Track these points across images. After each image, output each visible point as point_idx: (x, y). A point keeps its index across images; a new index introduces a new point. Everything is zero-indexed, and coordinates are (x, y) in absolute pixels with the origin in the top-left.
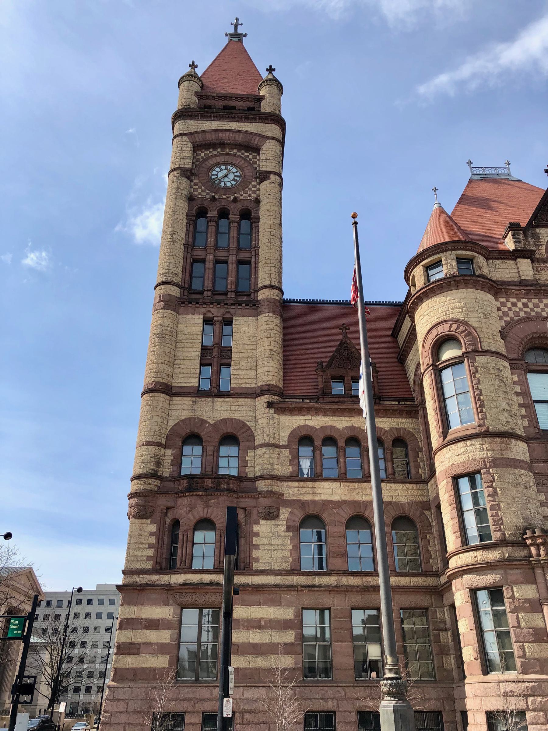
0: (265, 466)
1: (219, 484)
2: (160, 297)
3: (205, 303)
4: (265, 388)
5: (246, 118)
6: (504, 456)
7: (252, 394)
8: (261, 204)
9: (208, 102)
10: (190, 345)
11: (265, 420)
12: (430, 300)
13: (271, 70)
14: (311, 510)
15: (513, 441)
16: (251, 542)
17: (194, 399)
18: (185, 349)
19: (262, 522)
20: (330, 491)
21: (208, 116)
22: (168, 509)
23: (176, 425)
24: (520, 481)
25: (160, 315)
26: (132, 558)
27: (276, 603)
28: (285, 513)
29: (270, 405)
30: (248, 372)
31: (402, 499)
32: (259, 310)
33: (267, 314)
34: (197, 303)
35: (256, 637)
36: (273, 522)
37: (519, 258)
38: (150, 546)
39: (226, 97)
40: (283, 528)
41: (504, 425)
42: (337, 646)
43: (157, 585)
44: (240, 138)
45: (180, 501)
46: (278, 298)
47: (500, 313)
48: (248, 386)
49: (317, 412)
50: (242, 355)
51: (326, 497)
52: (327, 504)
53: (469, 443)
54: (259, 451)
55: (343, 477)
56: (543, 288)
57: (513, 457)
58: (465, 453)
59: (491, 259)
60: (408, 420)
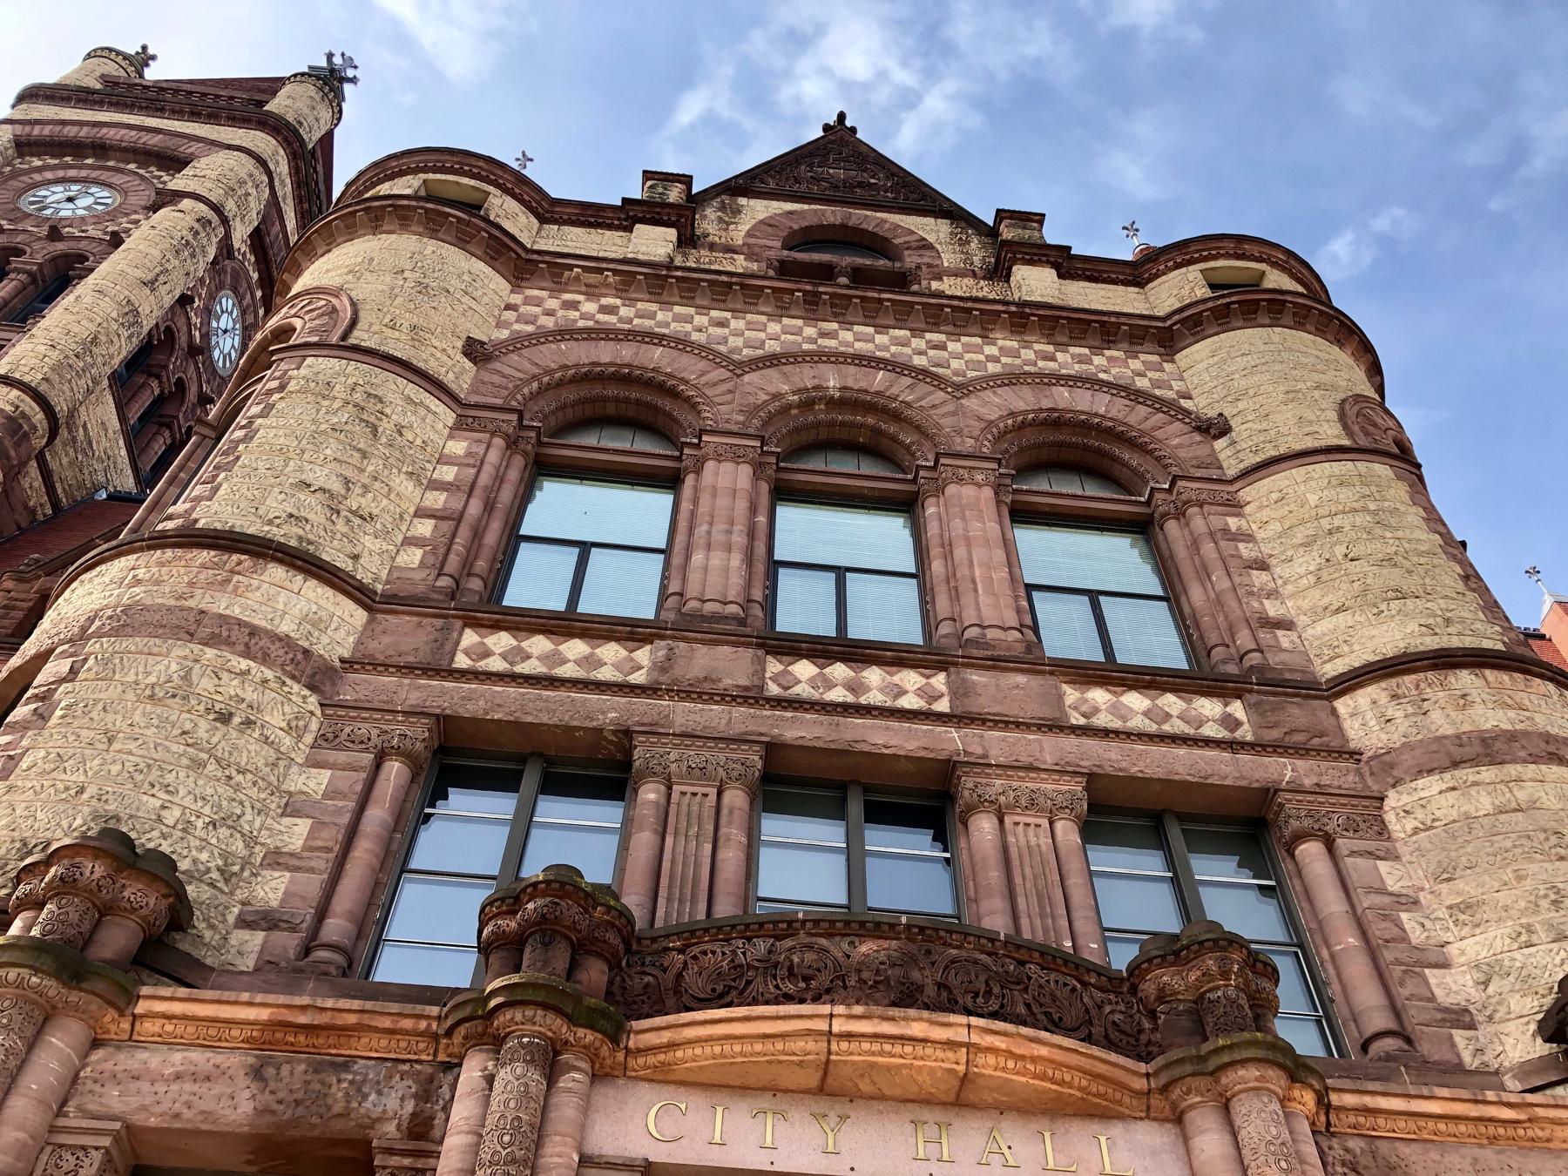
6: (191, 603)
15: (277, 572)
24: (205, 684)
37: (643, 221)
41: (270, 522)
46: (8, 408)
47: (510, 315)
56: (679, 274)
57: (236, 612)
59: (555, 222)
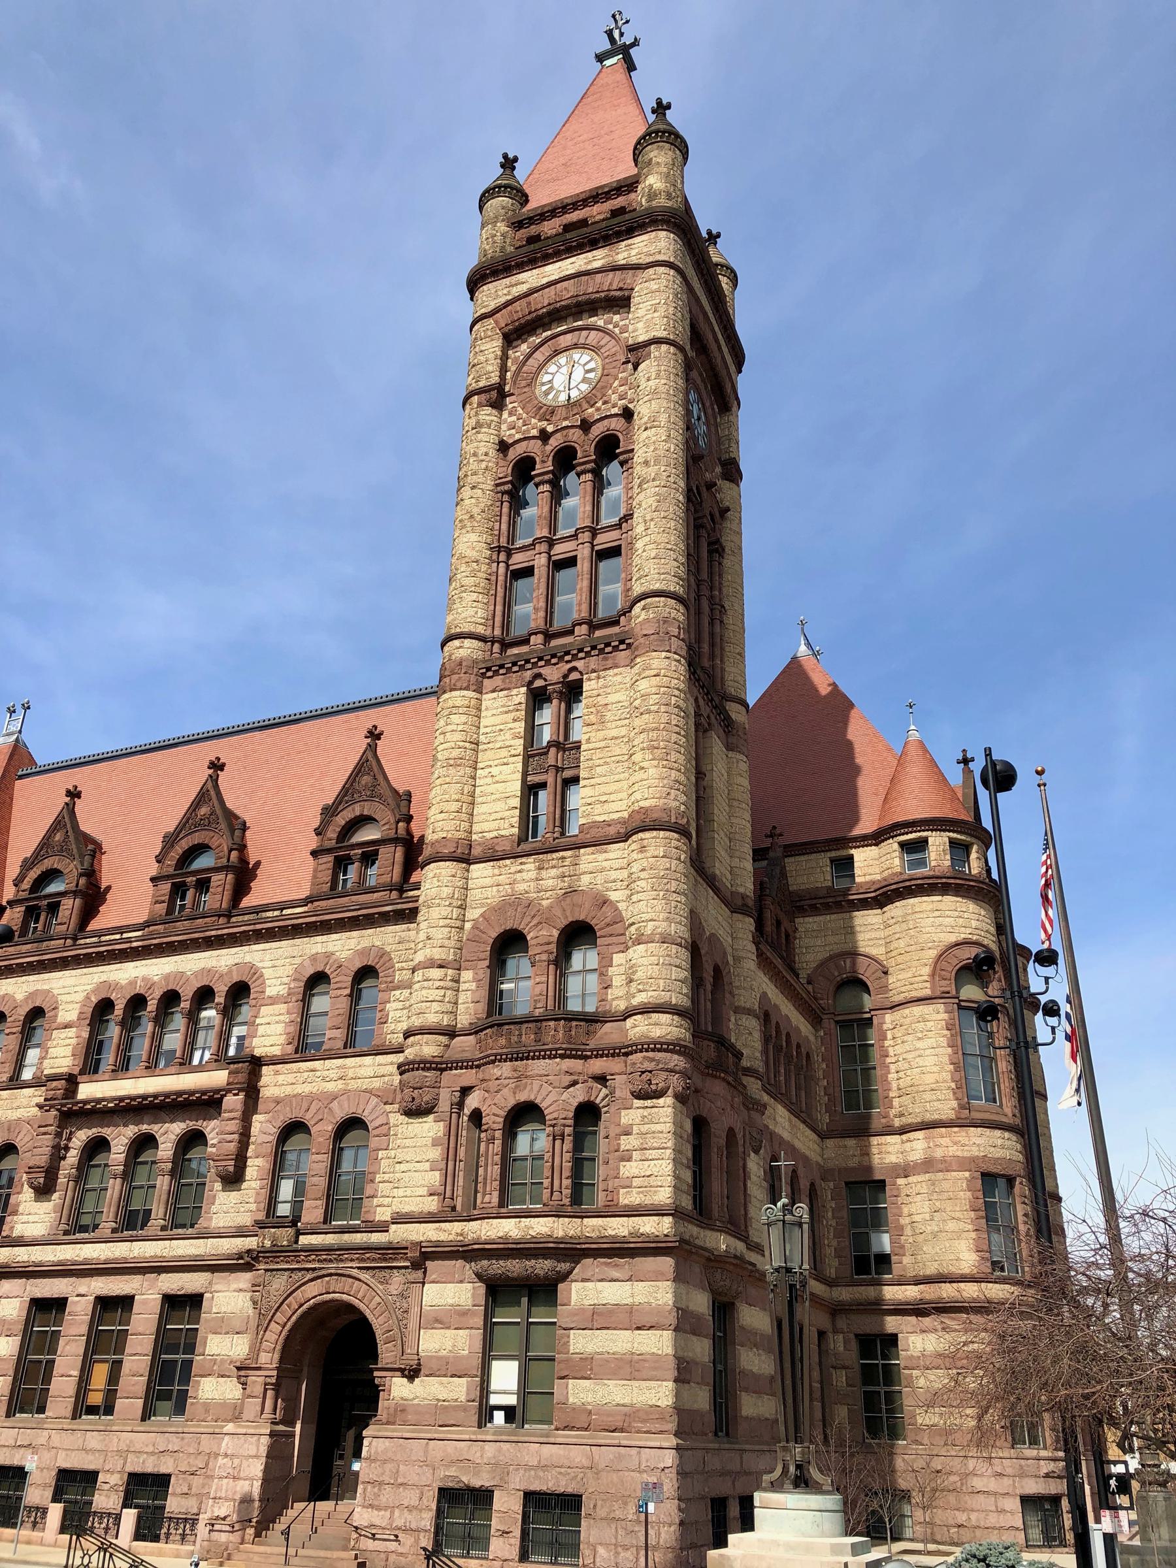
32: (733, 740)
35: (621, 1342)
60: (810, 1027)
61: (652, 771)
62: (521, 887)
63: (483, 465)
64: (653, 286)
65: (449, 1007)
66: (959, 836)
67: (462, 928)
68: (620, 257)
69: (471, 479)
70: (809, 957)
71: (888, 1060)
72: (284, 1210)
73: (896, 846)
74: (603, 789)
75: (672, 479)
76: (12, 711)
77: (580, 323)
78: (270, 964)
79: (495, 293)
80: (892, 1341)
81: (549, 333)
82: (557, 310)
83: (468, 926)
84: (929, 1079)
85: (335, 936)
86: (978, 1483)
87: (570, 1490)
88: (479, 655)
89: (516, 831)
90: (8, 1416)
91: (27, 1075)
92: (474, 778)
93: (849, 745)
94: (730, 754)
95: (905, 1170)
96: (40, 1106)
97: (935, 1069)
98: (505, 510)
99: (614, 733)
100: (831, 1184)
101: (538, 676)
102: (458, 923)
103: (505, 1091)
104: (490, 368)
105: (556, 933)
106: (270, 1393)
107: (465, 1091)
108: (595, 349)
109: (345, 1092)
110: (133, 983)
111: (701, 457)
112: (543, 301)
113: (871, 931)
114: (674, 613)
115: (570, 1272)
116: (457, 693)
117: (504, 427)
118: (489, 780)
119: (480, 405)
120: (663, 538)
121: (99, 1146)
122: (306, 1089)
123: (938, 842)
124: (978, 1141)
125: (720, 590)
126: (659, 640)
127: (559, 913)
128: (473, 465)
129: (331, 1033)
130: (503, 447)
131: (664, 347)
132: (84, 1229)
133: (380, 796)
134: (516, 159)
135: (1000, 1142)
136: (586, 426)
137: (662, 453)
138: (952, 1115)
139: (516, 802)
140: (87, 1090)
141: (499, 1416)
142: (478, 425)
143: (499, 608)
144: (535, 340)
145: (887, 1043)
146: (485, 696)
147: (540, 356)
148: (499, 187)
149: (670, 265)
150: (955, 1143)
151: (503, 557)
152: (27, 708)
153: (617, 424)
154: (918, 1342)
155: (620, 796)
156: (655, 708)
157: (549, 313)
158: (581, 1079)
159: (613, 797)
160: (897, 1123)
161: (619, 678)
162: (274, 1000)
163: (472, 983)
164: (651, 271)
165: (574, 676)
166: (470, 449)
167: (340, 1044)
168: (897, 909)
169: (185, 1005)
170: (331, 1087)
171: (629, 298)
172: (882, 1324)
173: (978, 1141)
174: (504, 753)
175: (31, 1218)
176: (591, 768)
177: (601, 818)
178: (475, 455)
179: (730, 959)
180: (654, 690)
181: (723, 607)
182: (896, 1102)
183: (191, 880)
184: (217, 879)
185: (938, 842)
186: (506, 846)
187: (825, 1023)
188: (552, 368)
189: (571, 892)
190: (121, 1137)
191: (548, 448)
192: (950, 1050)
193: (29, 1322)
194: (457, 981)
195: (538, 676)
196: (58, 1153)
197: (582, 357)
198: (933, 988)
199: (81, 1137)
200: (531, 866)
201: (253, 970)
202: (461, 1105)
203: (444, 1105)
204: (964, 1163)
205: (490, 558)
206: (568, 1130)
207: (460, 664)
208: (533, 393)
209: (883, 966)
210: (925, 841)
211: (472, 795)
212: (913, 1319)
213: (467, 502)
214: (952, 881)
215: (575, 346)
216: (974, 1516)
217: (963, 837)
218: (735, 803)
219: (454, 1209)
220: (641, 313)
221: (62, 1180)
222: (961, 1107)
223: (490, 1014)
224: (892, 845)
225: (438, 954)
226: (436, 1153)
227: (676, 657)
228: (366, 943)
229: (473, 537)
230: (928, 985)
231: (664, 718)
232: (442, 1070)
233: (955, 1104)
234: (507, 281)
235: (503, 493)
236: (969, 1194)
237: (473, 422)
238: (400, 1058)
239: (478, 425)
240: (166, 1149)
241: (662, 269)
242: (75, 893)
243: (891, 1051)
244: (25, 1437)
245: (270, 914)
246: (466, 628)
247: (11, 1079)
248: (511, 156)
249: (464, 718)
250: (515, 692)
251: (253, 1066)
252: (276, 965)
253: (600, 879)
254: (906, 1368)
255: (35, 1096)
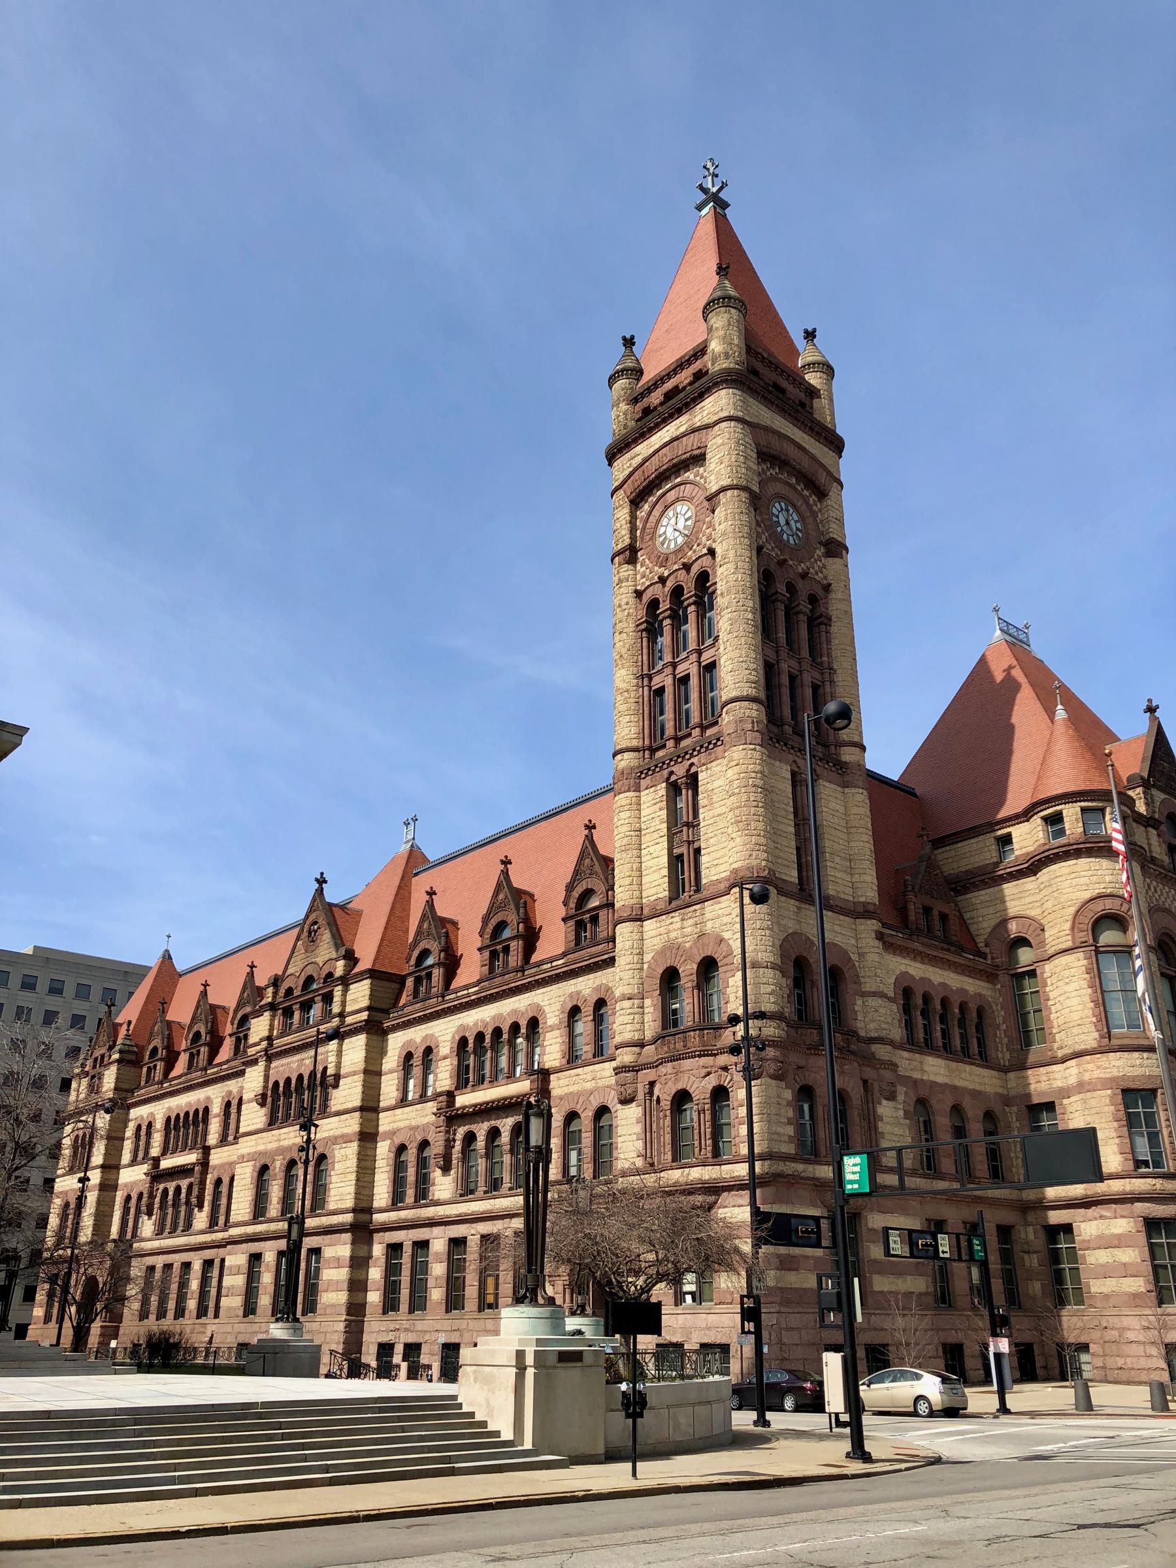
0: (883, 1026)
1: (848, 1042)
2: (753, 722)
3: (793, 748)
4: (871, 908)
5: (811, 428)
7: (859, 912)
8: (833, 596)
9: (759, 366)
10: (784, 813)
11: (876, 958)
12: (1092, 859)
13: (810, 335)
14: (924, 1092)
16: (876, 1128)
17: (797, 903)
18: (780, 819)
19: (884, 1102)
20: (934, 1069)
21: (770, 401)
22: (799, 1068)
23: (784, 940)
25: (757, 755)
26: (776, 1137)
27: (905, 1211)
28: (901, 1090)
29: (880, 936)
30: (844, 876)
31: (988, 1089)
33: (861, 791)
34: (786, 745)
36: (891, 1104)
38: (789, 1123)
39: (777, 367)
40: (901, 1113)
42: (958, 1268)
43: (803, 1178)
44: (805, 463)
45: (812, 1060)
48: (846, 897)
49: (917, 955)
50: (836, 846)
51: (932, 1078)
52: (934, 1084)
53: (1145, 1055)
54: (873, 1002)
55: (928, 1047)
58: (1141, 1066)
60: (986, 985)
61: (738, 840)
62: (673, 935)
63: (626, 613)
64: (719, 441)
65: (638, 1026)
66: (1090, 804)
67: (642, 969)
68: (697, 419)
69: (619, 626)
70: (985, 924)
71: (1050, 1003)
72: (573, 1171)
73: (1039, 821)
74: (714, 855)
75: (741, 604)
76: (407, 824)
77: (678, 480)
78: (546, 1003)
79: (625, 464)
80: (1068, 1229)
81: (661, 491)
82: (661, 474)
83: (645, 966)
84: (1075, 1016)
85: (581, 979)
86: (1131, 1336)
87: (723, 1342)
88: (635, 763)
89: (667, 893)
90: (447, 1312)
91: (429, 1093)
92: (640, 857)
93: (1012, 727)
94: (846, 790)
95: (1066, 1092)
96: (435, 1114)
97: (1080, 1007)
98: (645, 644)
99: (719, 811)
100: (1015, 1109)
101: (672, 773)
102: (639, 966)
103: (670, 1083)
104: (623, 532)
105: (695, 966)
106: (567, 1291)
107: (652, 1084)
108: (690, 500)
109: (597, 1089)
110: (476, 1024)
111: (786, 560)
112: (652, 467)
113: (1021, 899)
114: (748, 712)
115: (715, 1203)
116: (622, 796)
117: (638, 577)
118: (649, 857)
119: (620, 564)
120: (737, 653)
121: (470, 1138)
122: (575, 1088)
123: (1071, 813)
124: (1117, 1063)
125: (829, 655)
126: (740, 737)
127: (695, 951)
128: (620, 615)
129: (585, 1048)
130: (639, 594)
131: (729, 493)
132: (472, 1192)
133: (596, 873)
134: (633, 337)
135: (1138, 1062)
136: (687, 567)
137: (731, 584)
138: (1094, 1044)
139: (665, 872)
140: (464, 1100)
141: (689, 1298)
142: (620, 581)
143: (646, 723)
144: (652, 499)
145: (1048, 989)
146: (643, 793)
147: (656, 513)
148: (618, 372)
149: (730, 418)
150: (1098, 1067)
151: (646, 681)
152: (415, 820)
153: (706, 561)
154: (1088, 1226)
155: (726, 859)
156: (737, 791)
157: (657, 477)
158: (713, 1070)
159: (721, 861)
160: (1060, 1054)
161: (719, 768)
162: (552, 1028)
163: (651, 1006)
164: (717, 428)
165: (693, 770)
166: (616, 602)
167: (590, 1055)
168: (1046, 874)
169: (505, 1036)
170: (589, 1086)
171: (704, 454)
172: (1046, 1218)
173: (1117, 1063)
174: (656, 835)
175: (442, 1187)
176: (707, 840)
177: (714, 878)
178: (620, 606)
179: (854, 957)
180: (736, 777)
181: (831, 669)
182: (1058, 1037)
183: (499, 947)
184: (513, 944)
185: (1071, 813)
186: (662, 906)
187: (1001, 978)
188: (664, 521)
189: (702, 935)
190: (481, 1130)
191: (667, 589)
192: (1090, 990)
193: (450, 1253)
194: (642, 1007)
195: (672, 773)
196: (449, 1144)
197: (681, 508)
198: (1074, 942)
199: (461, 1131)
200: (677, 919)
201: (539, 1008)
202: (651, 1093)
203: (640, 1096)
204: (1108, 1083)
205: (637, 685)
206: (707, 1107)
207: (623, 773)
208: (654, 544)
209: (1041, 924)
210: (1060, 813)
211: (640, 870)
212: (1082, 1211)
213: (617, 645)
214: (1082, 846)
215: (678, 500)
216: (1129, 1360)
217: (1094, 804)
218: (853, 830)
219: (652, 1165)
220: (712, 466)
221: (454, 1162)
222: (1102, 1037)
223: (664, 1027)
224: (1037, 820)
225: (627, 990)
226: (639, 1128)
227: (752, 747)
228: (598, 983)
229: (623, 672)
230: (1069, 937)
231: (745, 797)
232: (637, 1071)
233: (1096, 1035)
234: (628, 456)
235: (642, 631)
236: (1112, 1108)
237: (616, 579)
238: (614, 1064)
239: (620, 581)
240: (505, 1138)
241: (724, 425)
242: (439, 964)
243: (1052, 995)
244: (456, 1324)
245: (545, 967)
246: (624, 745)
247: (421, 1097)
248: (628, 336)
249: (628, 814)
250: (659, 787)
251: (544, 1075)
252: (549, 1002)
253: (718, 923)
254: (1080, 1249)
255: (431, 1106)
